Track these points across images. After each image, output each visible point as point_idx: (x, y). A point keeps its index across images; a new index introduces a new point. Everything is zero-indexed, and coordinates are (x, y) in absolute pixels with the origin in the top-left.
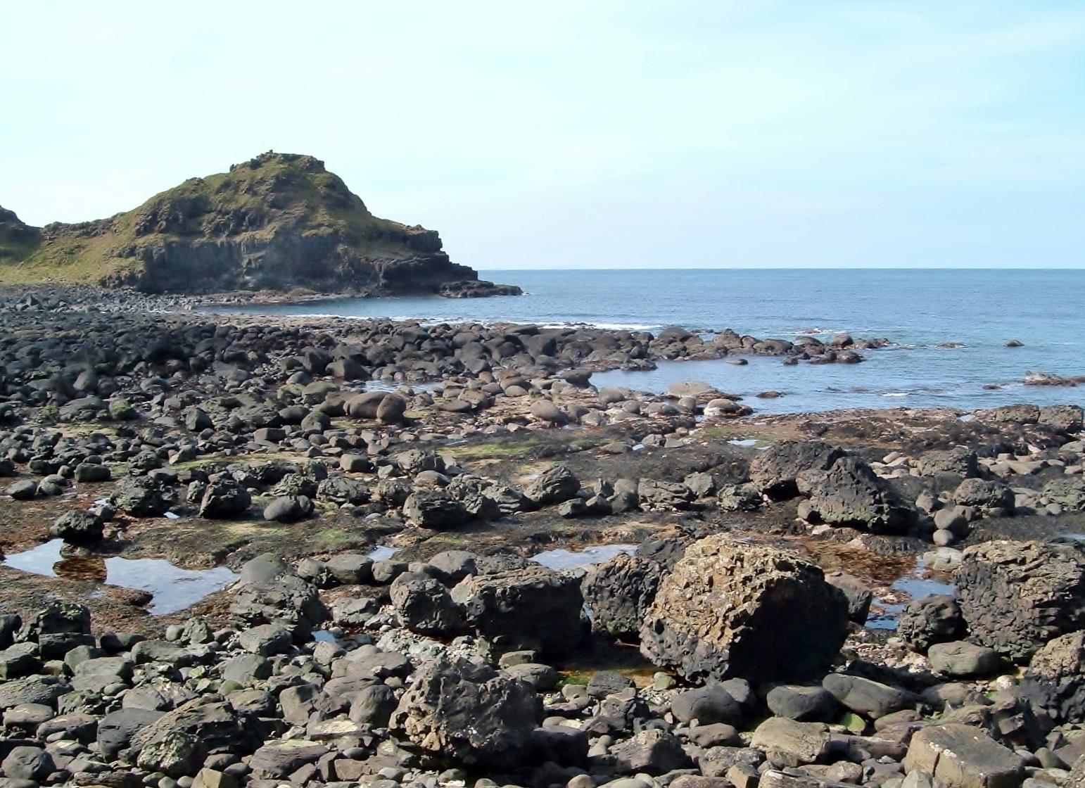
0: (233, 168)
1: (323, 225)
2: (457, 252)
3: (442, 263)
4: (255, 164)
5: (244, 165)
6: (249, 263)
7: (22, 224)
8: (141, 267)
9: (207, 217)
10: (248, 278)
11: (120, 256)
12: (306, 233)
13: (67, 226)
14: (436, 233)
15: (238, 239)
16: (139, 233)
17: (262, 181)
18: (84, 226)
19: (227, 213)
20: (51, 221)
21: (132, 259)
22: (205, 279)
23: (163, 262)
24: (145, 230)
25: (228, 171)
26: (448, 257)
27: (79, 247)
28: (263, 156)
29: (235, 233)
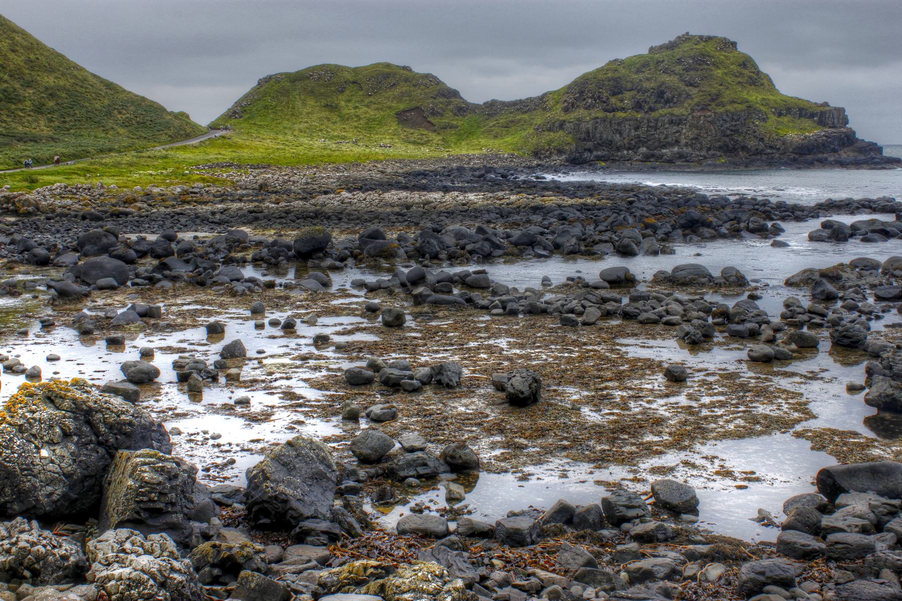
0: (652, 50)
1: (735, 102)
2: (864, 127)
3: (849, 139)
4: (671, 46)
5: (661, 47)
7: (465, 102)
8: (569, 139)
10: (664, 151)
11: (550, 130)
12: (720, 110)
13: (504, 104)
14: (841, 111)
16: (566, 110)
17: (679, 61)
18: (514, 104)
19: (647, 91)
20: (489, 99)
21: (561, 133)
22: (625, 152)
23: (588, 136)
25: (647, 52)
26: (854, 133)
28: (679, 37)
29: (652, 109)
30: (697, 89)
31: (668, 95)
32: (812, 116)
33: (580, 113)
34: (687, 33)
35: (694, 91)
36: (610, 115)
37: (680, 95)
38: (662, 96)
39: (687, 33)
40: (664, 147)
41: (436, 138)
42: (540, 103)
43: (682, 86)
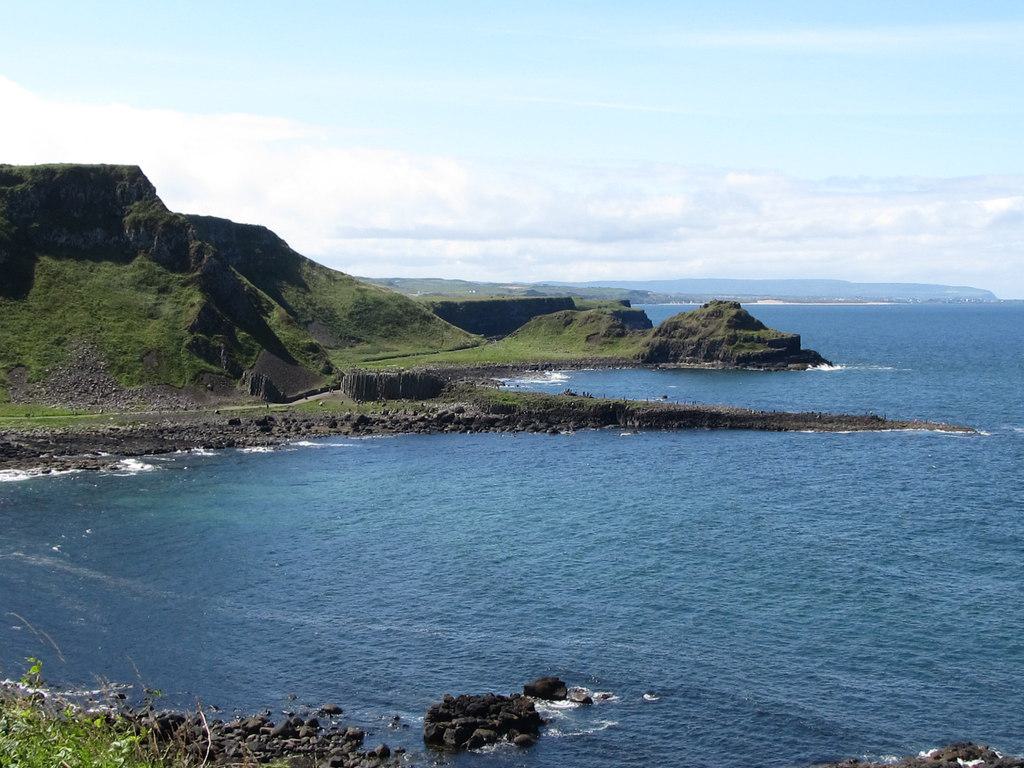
33: (658, 338)
35: (703, 329)
38: (692, 332)
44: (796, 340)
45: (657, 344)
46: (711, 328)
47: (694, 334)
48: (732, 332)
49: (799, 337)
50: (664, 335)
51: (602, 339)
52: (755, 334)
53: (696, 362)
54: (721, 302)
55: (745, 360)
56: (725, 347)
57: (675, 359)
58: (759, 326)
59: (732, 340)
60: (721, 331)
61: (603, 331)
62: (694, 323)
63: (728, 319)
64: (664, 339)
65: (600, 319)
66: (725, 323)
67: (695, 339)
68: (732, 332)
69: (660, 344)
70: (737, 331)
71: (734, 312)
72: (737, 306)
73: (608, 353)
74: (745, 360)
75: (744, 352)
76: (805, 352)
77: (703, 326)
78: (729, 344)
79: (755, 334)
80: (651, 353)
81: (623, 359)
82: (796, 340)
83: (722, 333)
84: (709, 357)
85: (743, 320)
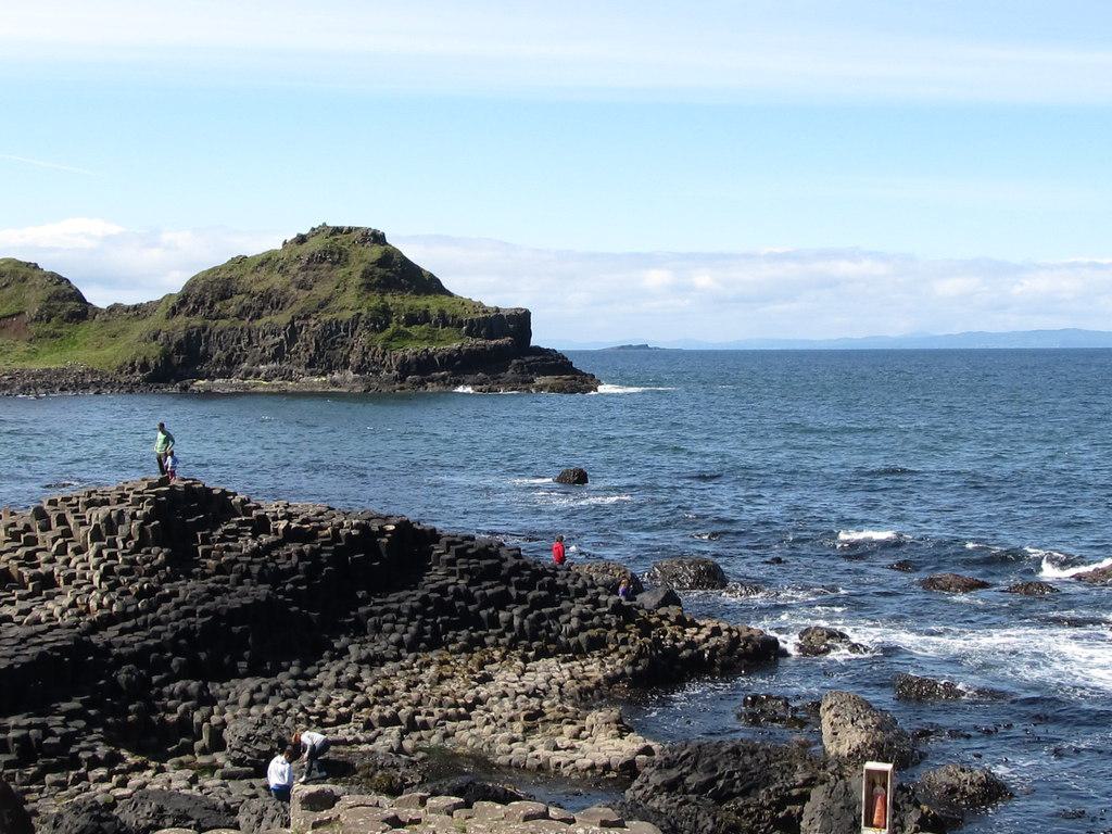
0: (285, 243)
6: (264, 351)
9: (237, 299)
12: (327, 318)
15: (258, 323)
18: (135, 308)
24: (174, 312)
25: (280, 247)
27: (123, 330)
29: (259, 317)
30: (308, 293)
31: (274, 299)
32: (461, 324)
33: (181, 320)
34: (324, 224)
35: (303, 295)
36: (211, 323)
37: (286, 300)
38: (270, 301)
39: (324, 224)
40: (264, 361)
41: (22, 347)
42: (138, 311)
43: (293, 289)
44: (520, 322)
45: (180, 335)
46: (322, 291)
47: (278, 305)
48: (375, 301)
49: (527, 314)
50: (195, 311)
51: (33, 328)
52: (432, 304)
53: (288, 376)
54: (337, 230)
55: (422, 368)
56: (362, 338)
57: (230, 366)
58: (432, 285)
59: (380, 319)
60: (350, 298)
61: (33, 309)
62: (276, 281)
63: (362, 267)
64: (197, 321)
65: (24, 279)
66: (356, 279)
67: (282, 319)
68: (375, 301)
69: (189, 335)
70: (389, 298)
71: (375, 252)
72: (378, 238)
73: (48, 361)
74: (422, 368)
75: (411, 349)
76: (538, 351)
77: (302, 286)
78: (373, 329)
79: (421, 302)
80: (166, 357)
81: (93, 372)
82: (520, 322)
83: (350, 303)
84: (322, 361)
85: (399, 274)
